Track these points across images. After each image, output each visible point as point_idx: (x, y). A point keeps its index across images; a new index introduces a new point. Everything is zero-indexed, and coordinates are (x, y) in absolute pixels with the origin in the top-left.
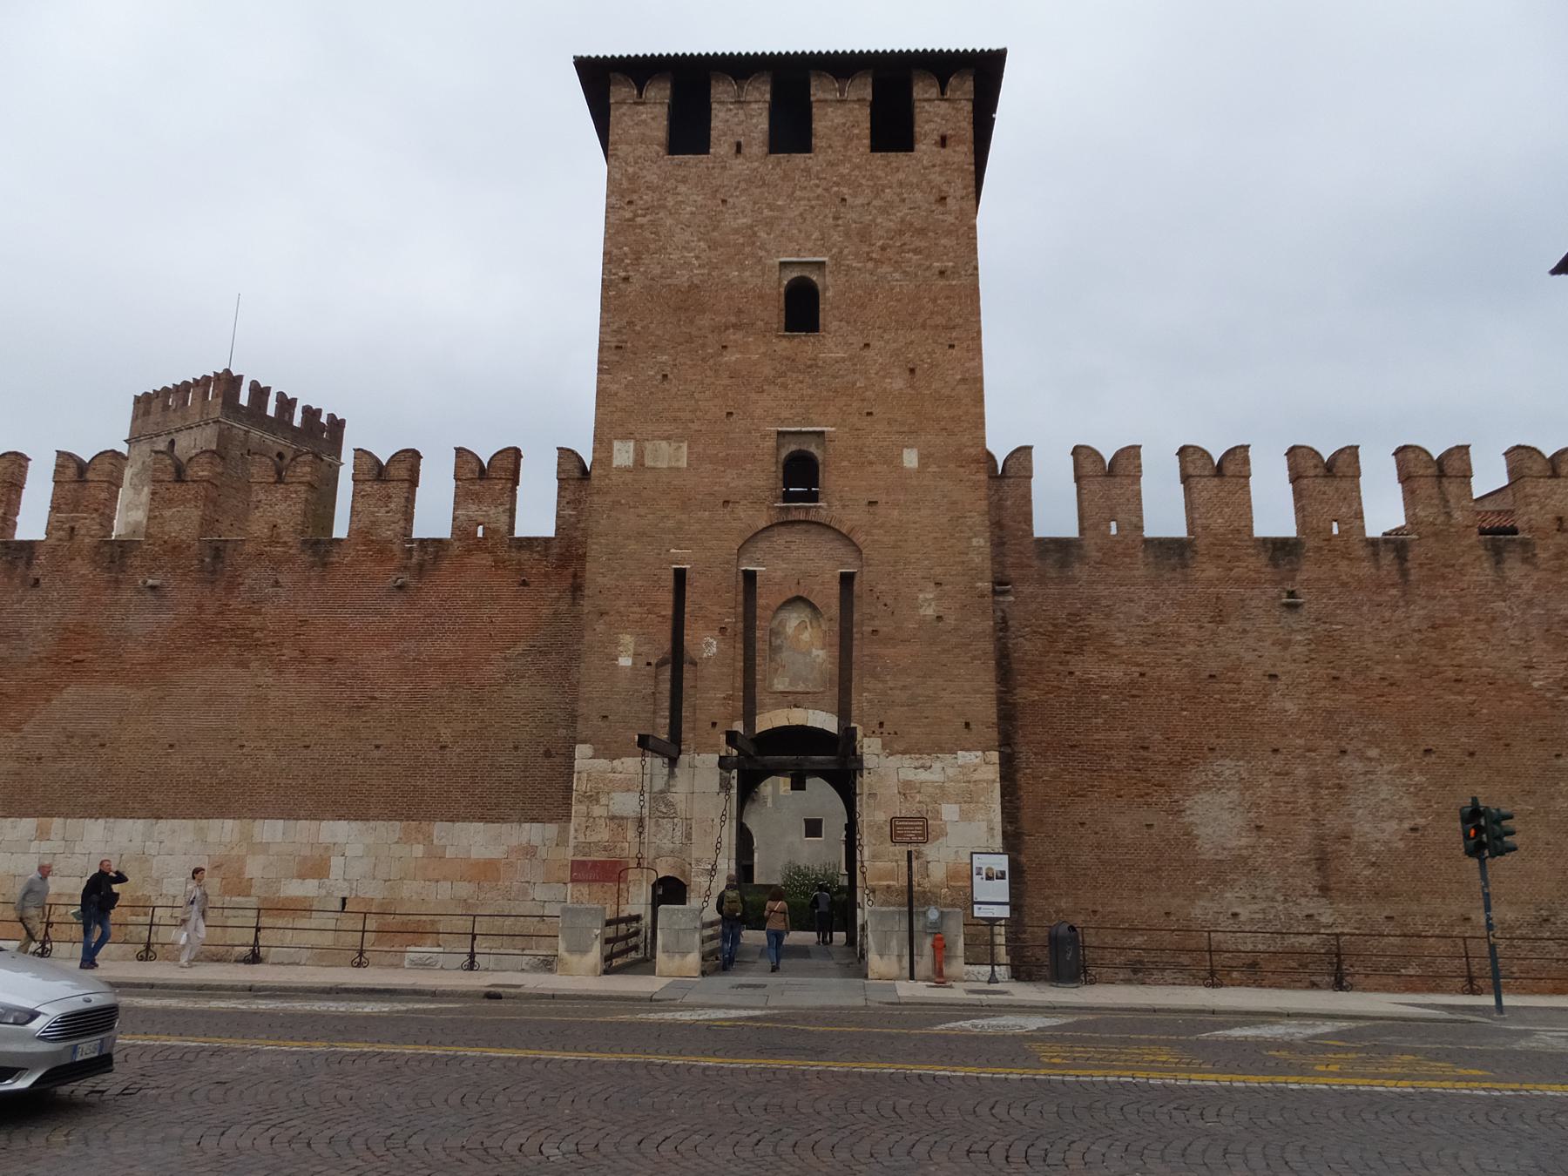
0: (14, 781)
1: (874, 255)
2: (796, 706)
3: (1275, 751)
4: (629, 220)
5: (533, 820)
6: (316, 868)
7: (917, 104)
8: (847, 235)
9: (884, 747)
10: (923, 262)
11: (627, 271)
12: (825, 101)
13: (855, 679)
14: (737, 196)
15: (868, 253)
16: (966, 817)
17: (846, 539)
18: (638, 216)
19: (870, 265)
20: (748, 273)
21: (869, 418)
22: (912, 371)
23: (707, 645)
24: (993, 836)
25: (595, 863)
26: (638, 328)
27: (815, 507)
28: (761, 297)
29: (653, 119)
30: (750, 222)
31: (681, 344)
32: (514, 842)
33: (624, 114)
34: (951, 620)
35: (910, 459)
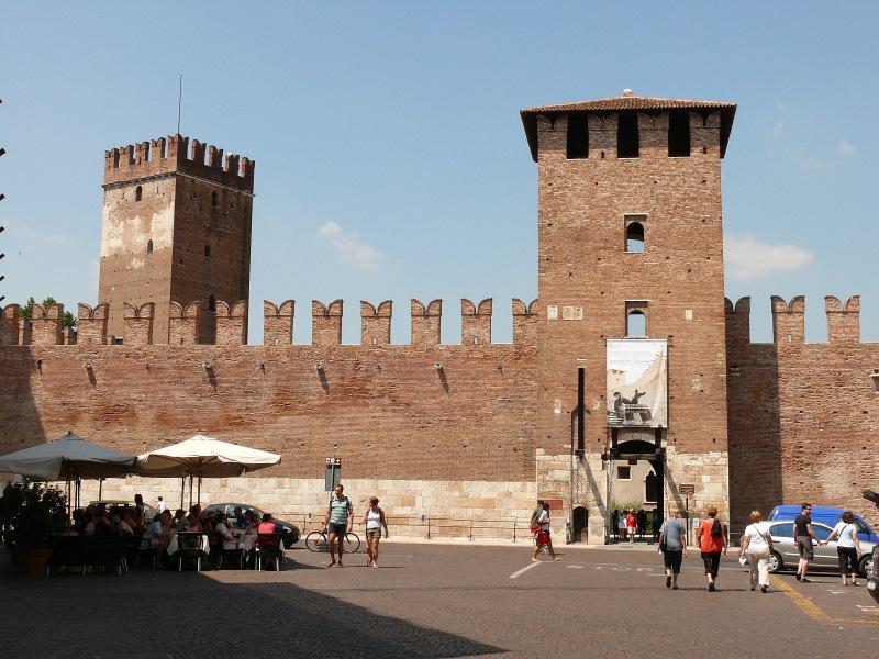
5: (510, 480)
6: (411, 503)
9: (676, 450)
19: (669, 216)
32: (501, 490)
35: (689, 315)
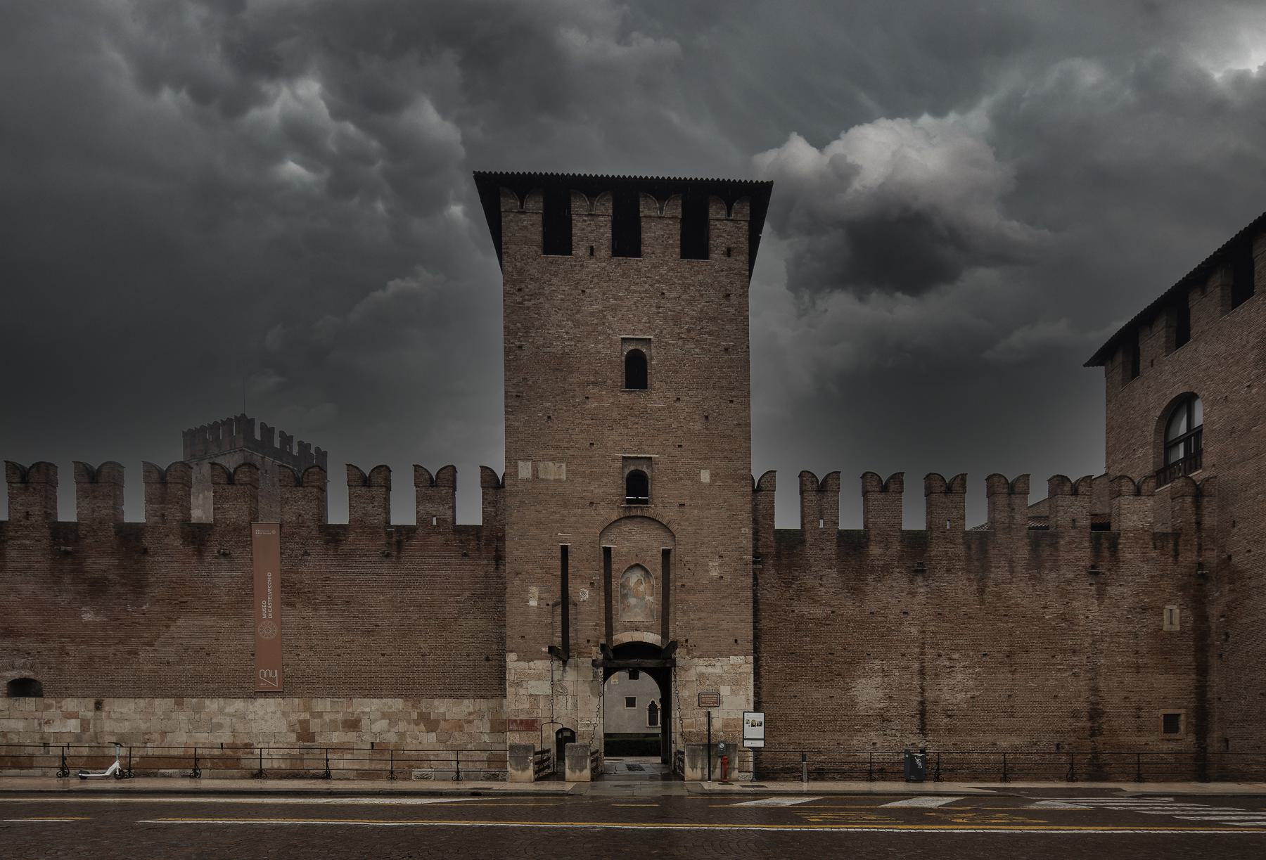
0: (155, 676)
1: (683, 336)
2: (636, 630)
3: (903, 655)
4: (520, 303)
7: (712, 222)
8: (665, 319)
10: (714, 341)
11: (521, 341)
12: (650, 217)
13: (671, 615)
14: (592, 288)
15: (679, 334)
16: (734, 693)
17: (666, 528)
18: (525, 300)
19: (680, 342)
20: (600, 346)
21: (680, 449)
22: (707, 417)
23: (583, 594)
24: (749, 703)
25: (522, 721)
26: (530, 383)
27: (647, 507)
28: (610, 363)
29: (532, 225)
30: (601, 308)
31: (559, 395)
33: (512, 221)
34: (728, 579)
35: (705, 476)
